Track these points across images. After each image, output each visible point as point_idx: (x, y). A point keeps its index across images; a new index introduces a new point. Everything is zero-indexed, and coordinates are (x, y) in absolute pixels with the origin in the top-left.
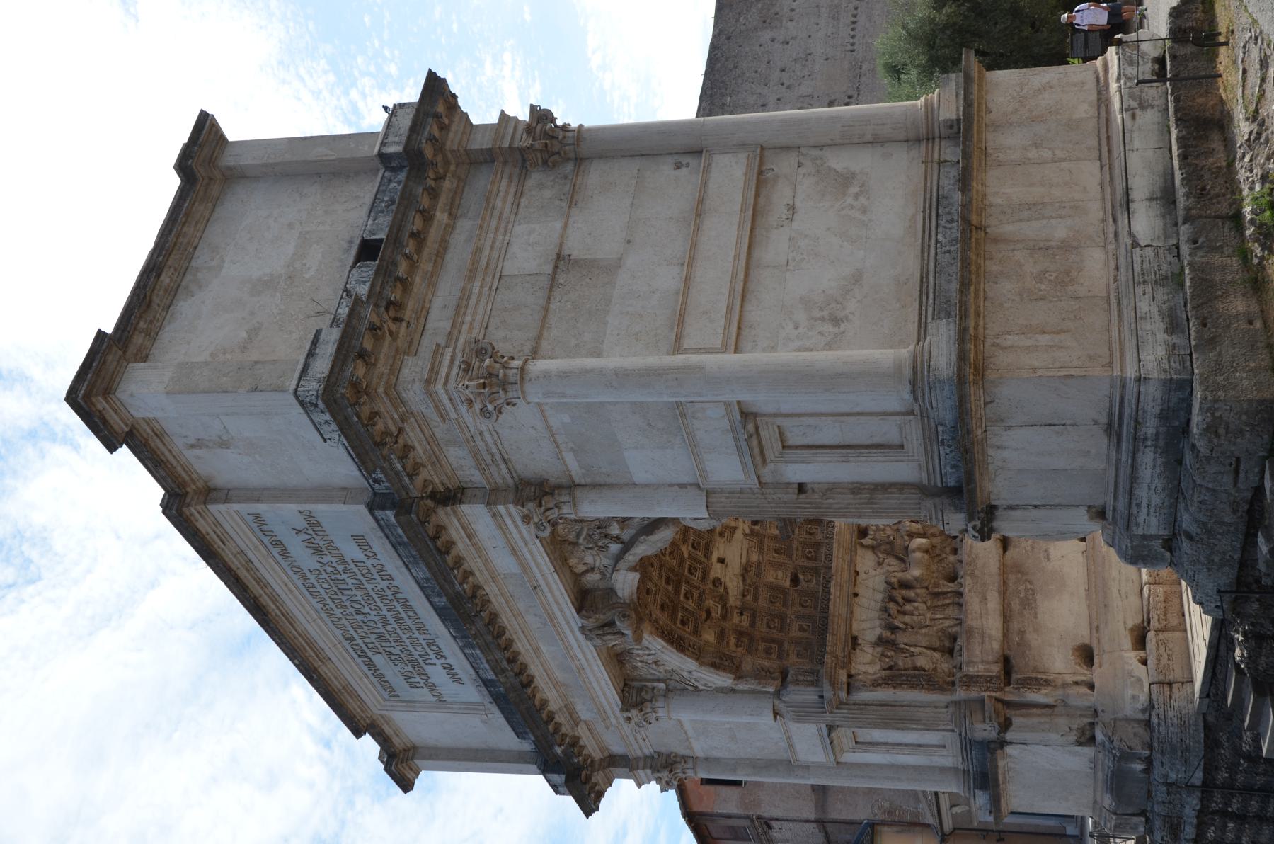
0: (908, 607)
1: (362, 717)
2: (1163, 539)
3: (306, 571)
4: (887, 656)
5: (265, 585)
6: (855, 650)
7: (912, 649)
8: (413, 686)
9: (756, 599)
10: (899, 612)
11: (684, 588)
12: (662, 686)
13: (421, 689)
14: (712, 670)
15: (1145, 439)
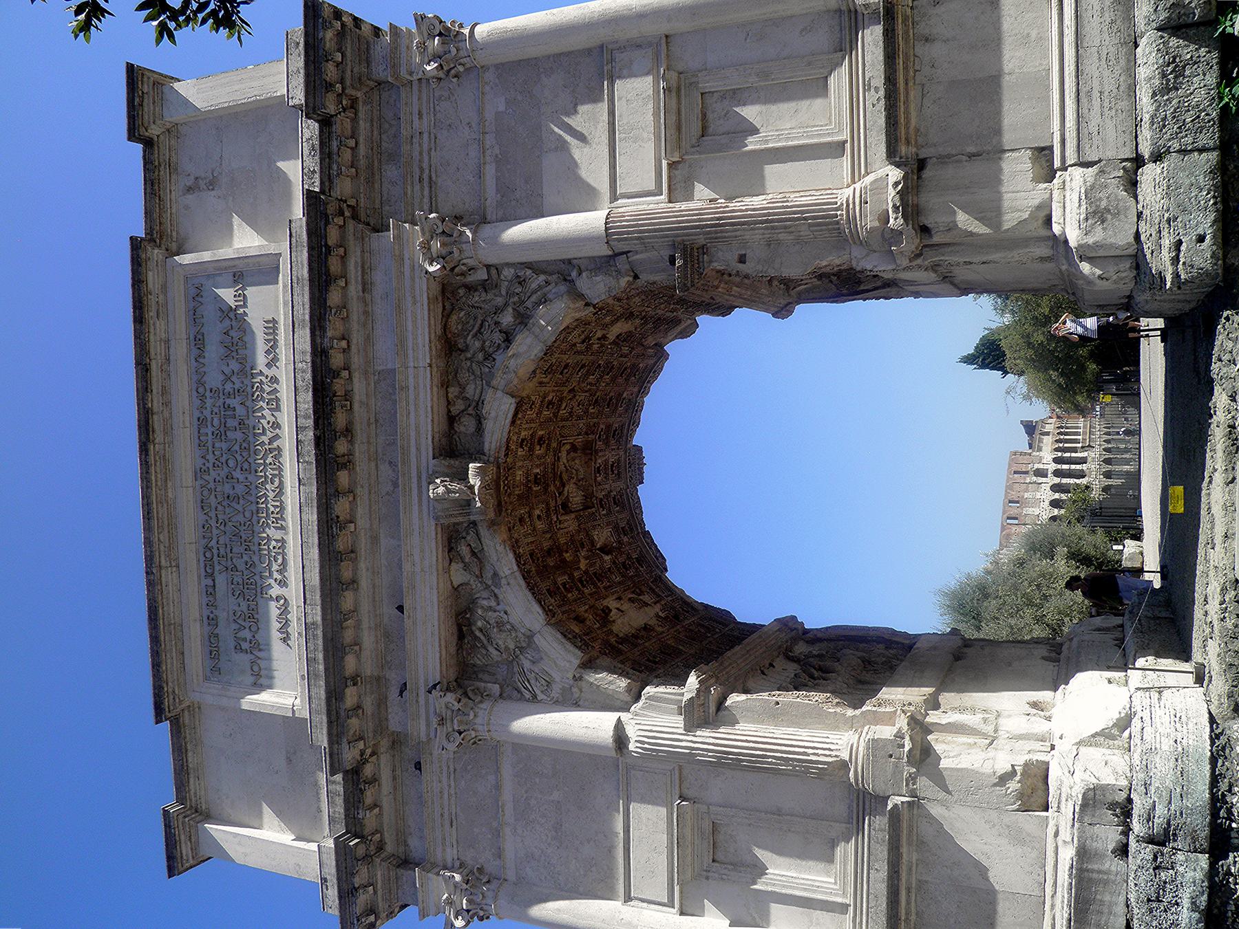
2: (1124, 168)
5: (167, 404)
14: (559, 636)
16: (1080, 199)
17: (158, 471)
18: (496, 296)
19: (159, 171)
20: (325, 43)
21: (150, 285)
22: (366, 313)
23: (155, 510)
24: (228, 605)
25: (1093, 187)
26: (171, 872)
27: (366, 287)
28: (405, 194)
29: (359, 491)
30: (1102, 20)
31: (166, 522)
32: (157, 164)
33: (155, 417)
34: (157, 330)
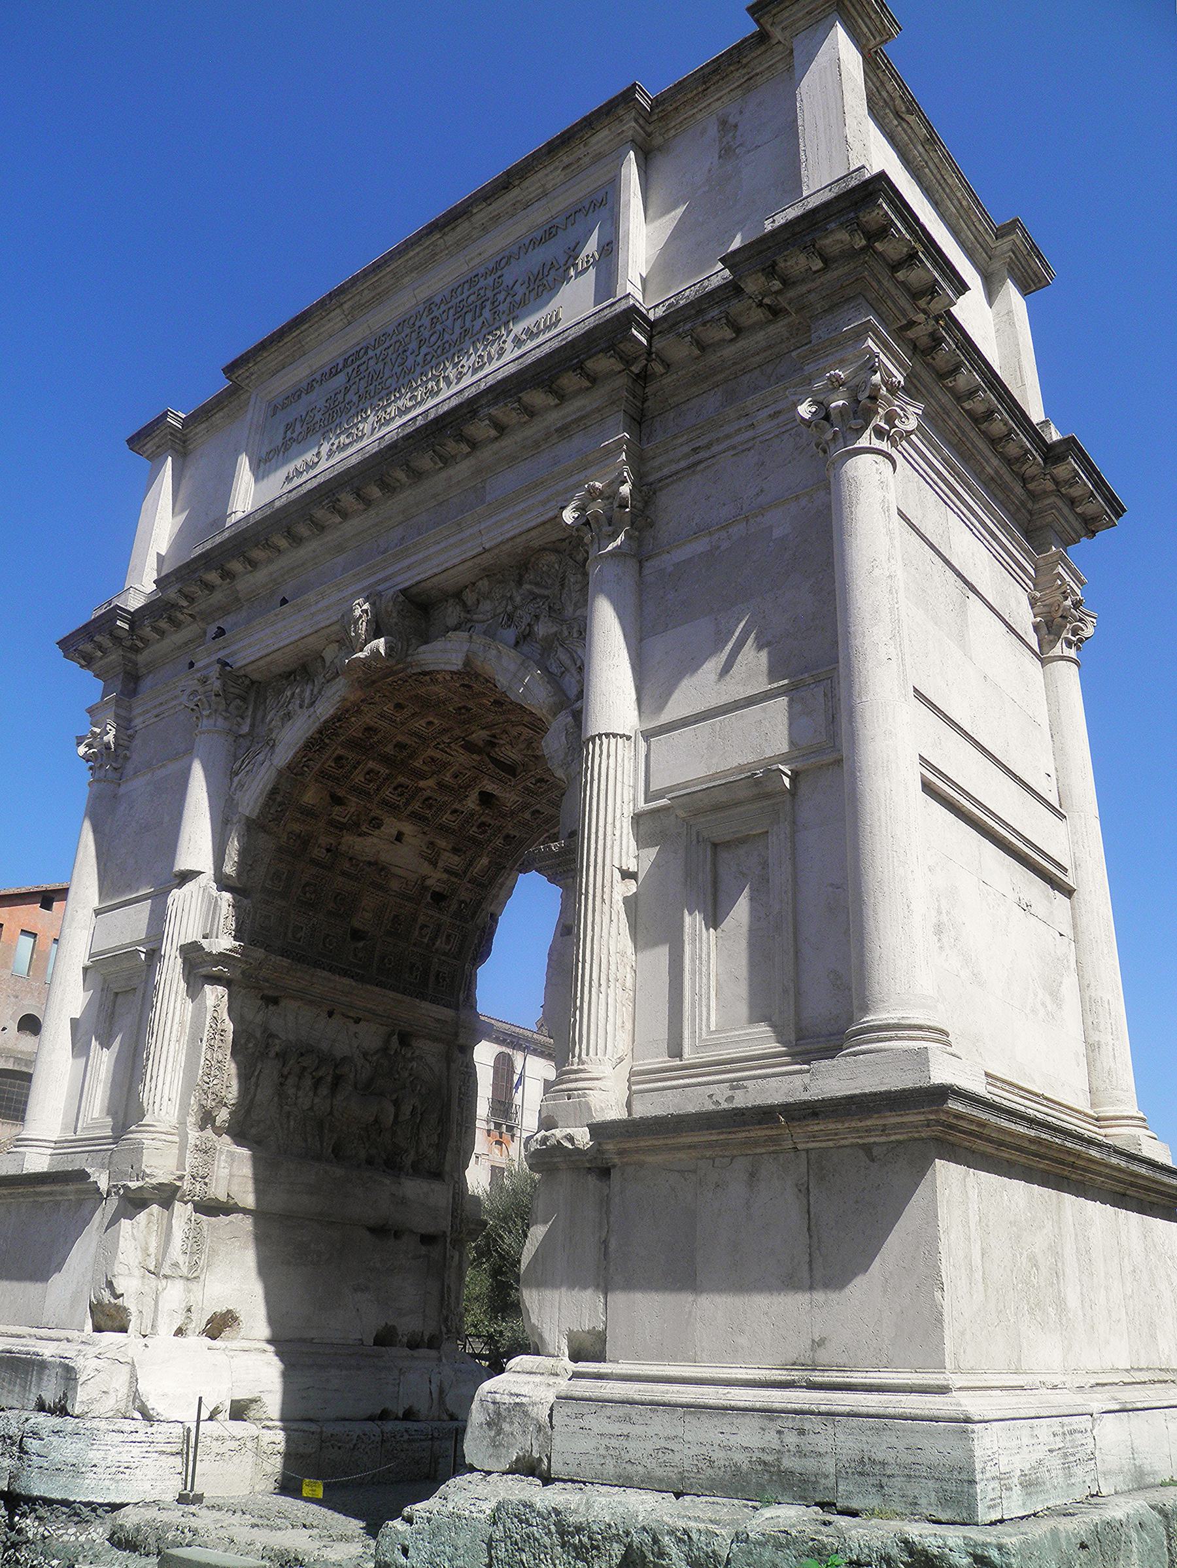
0: (308, 1082)
1: (252, 374)
2: (540, 1460)
3: (499, 273)
4: (248, 1040)
5: (485, 229)
6: (262, 998)
7: (253, 1080)
8: (288, 427)
9: (344, 873)
10: (304, 1068)
11: (384, 771)
12: (245, 729)
13: (282, 436)
14: (269, 787)
15: (802, 1432)
16: (518, 1395)
17: (421, 255)
18: (575, 605)
19: (737, 70)
20: (826, 237)
21: (594, 140)
22: (537, 444)
23: (384, 272)
24: (318, 397)
25: (526, 1414)
26: (131, 441)
27: (564, 431)
28: (675, 437)
29: (372, 512)
30: (716, 1447)
31: (380, 290)
32: (744, 61)
33: (466, 224)
34: (550, 176)
